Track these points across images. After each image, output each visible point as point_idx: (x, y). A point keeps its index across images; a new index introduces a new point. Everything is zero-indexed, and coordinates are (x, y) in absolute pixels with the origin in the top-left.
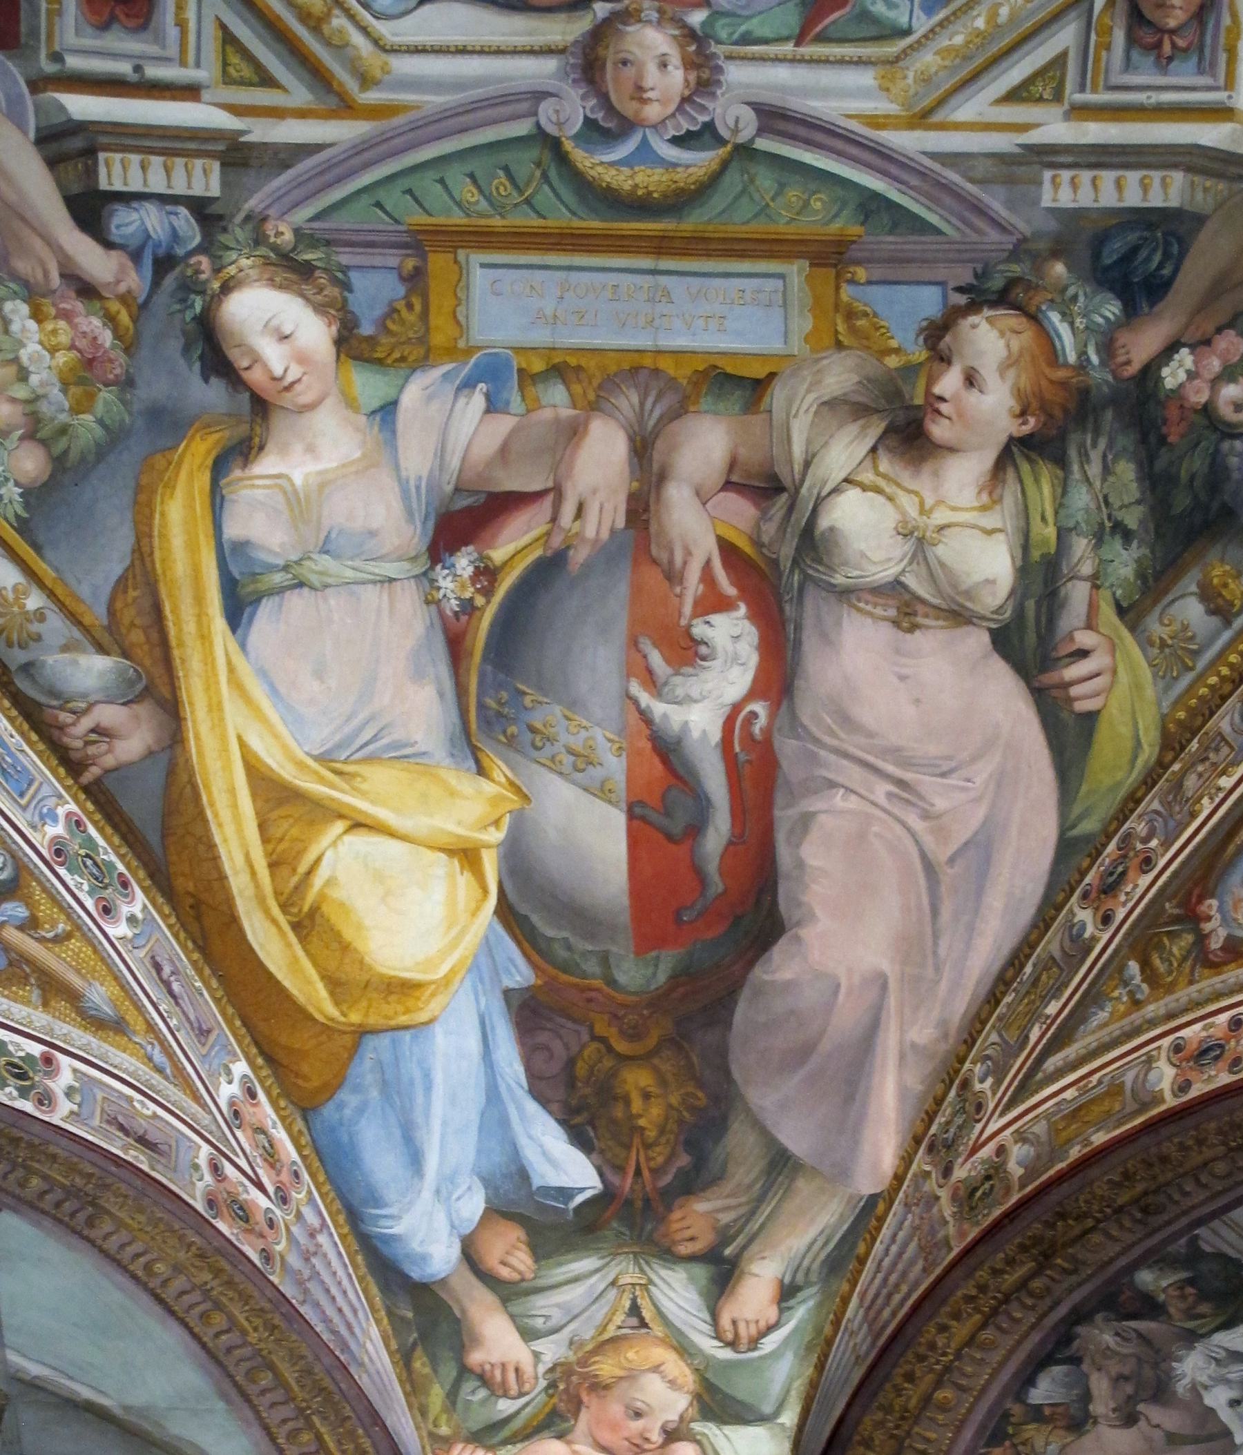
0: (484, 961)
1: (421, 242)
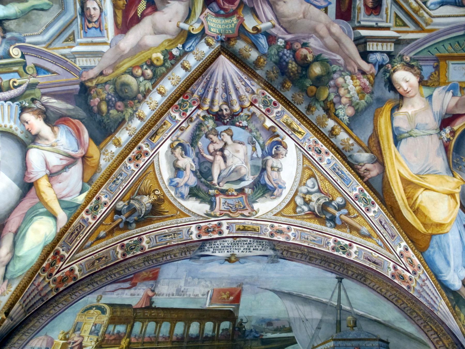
0: (458, 219)
1: (438, 59)
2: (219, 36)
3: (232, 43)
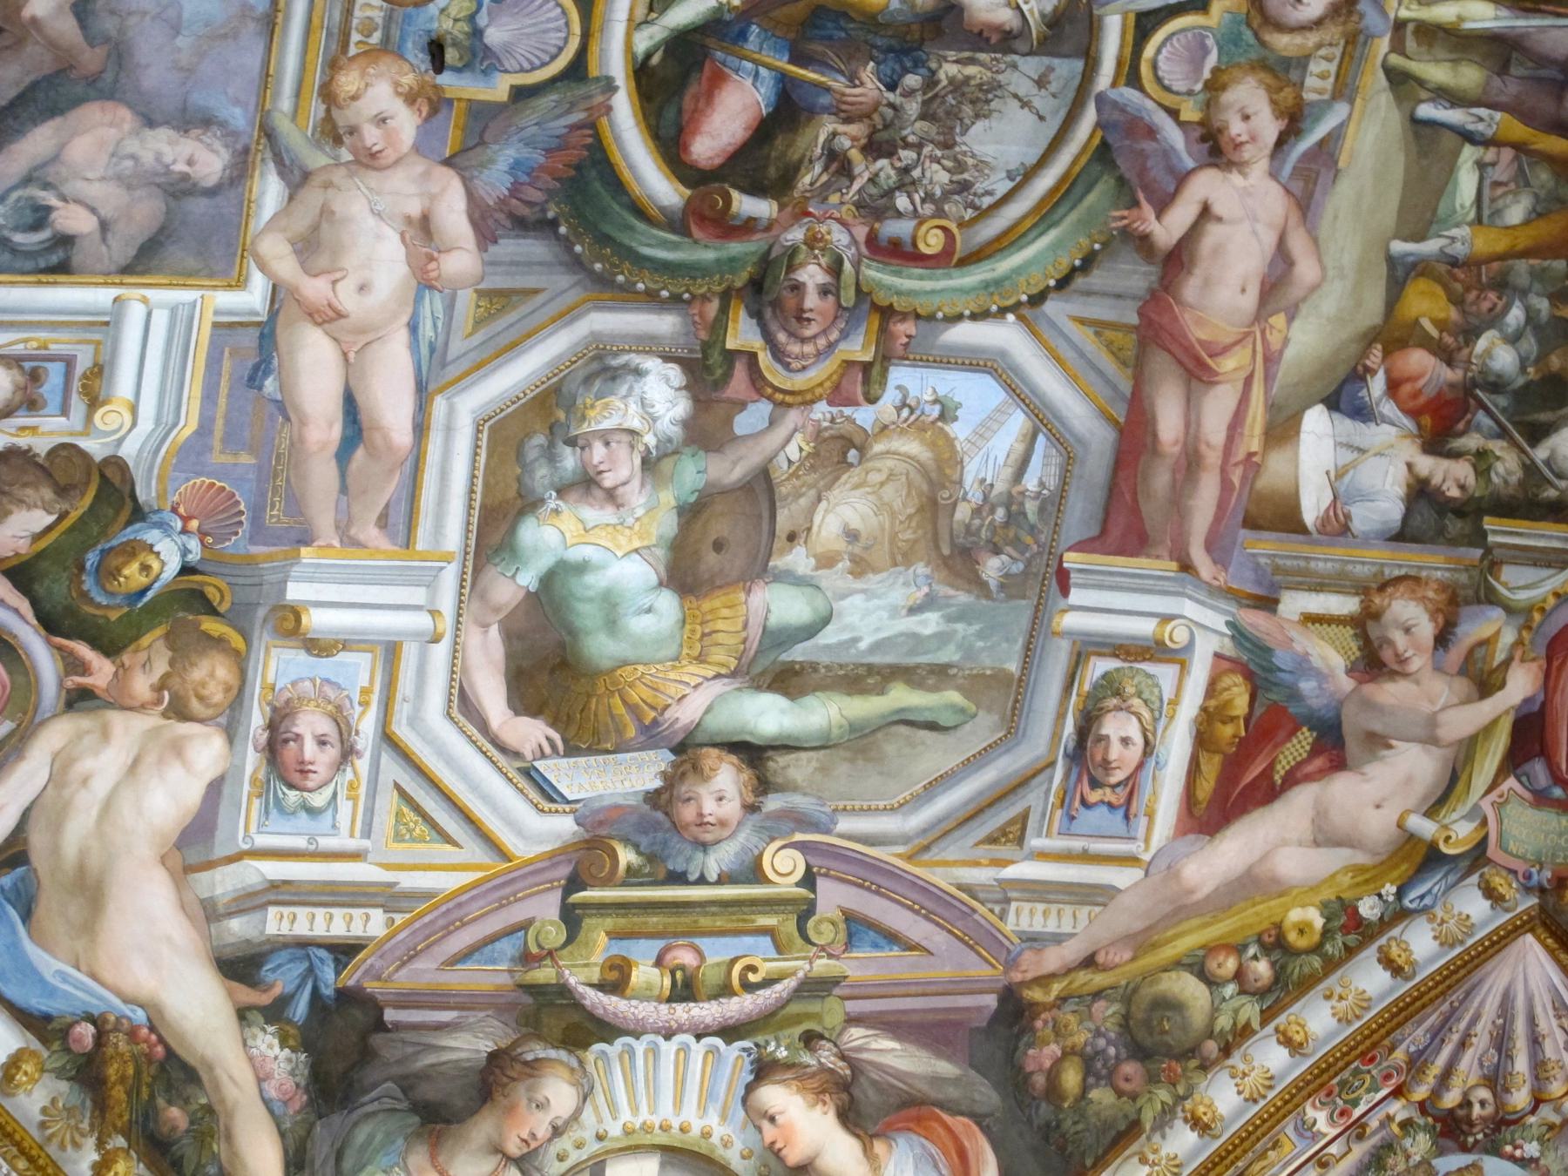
2: (1534, 870)
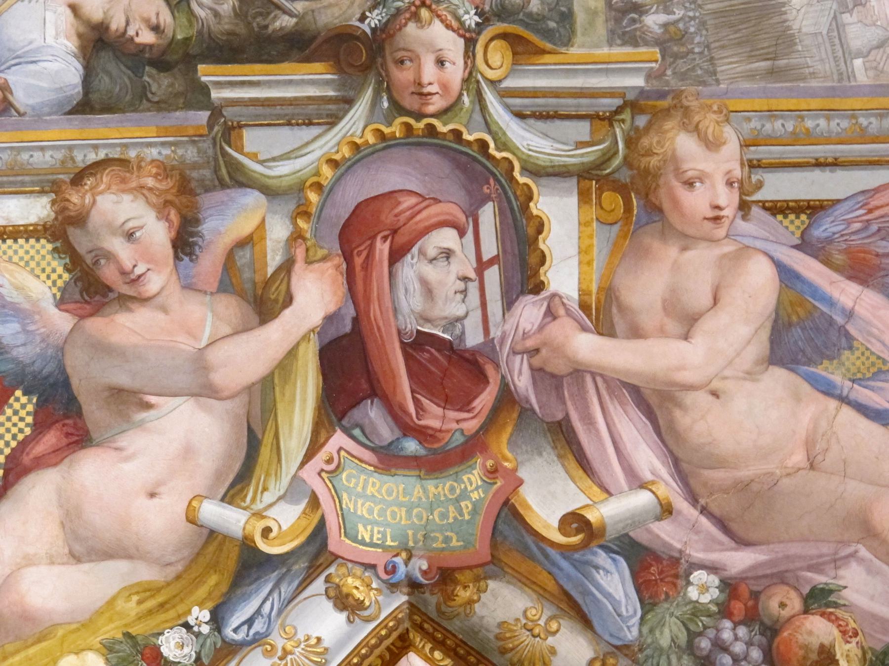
2: (398, 560)
3: (463, 594)
